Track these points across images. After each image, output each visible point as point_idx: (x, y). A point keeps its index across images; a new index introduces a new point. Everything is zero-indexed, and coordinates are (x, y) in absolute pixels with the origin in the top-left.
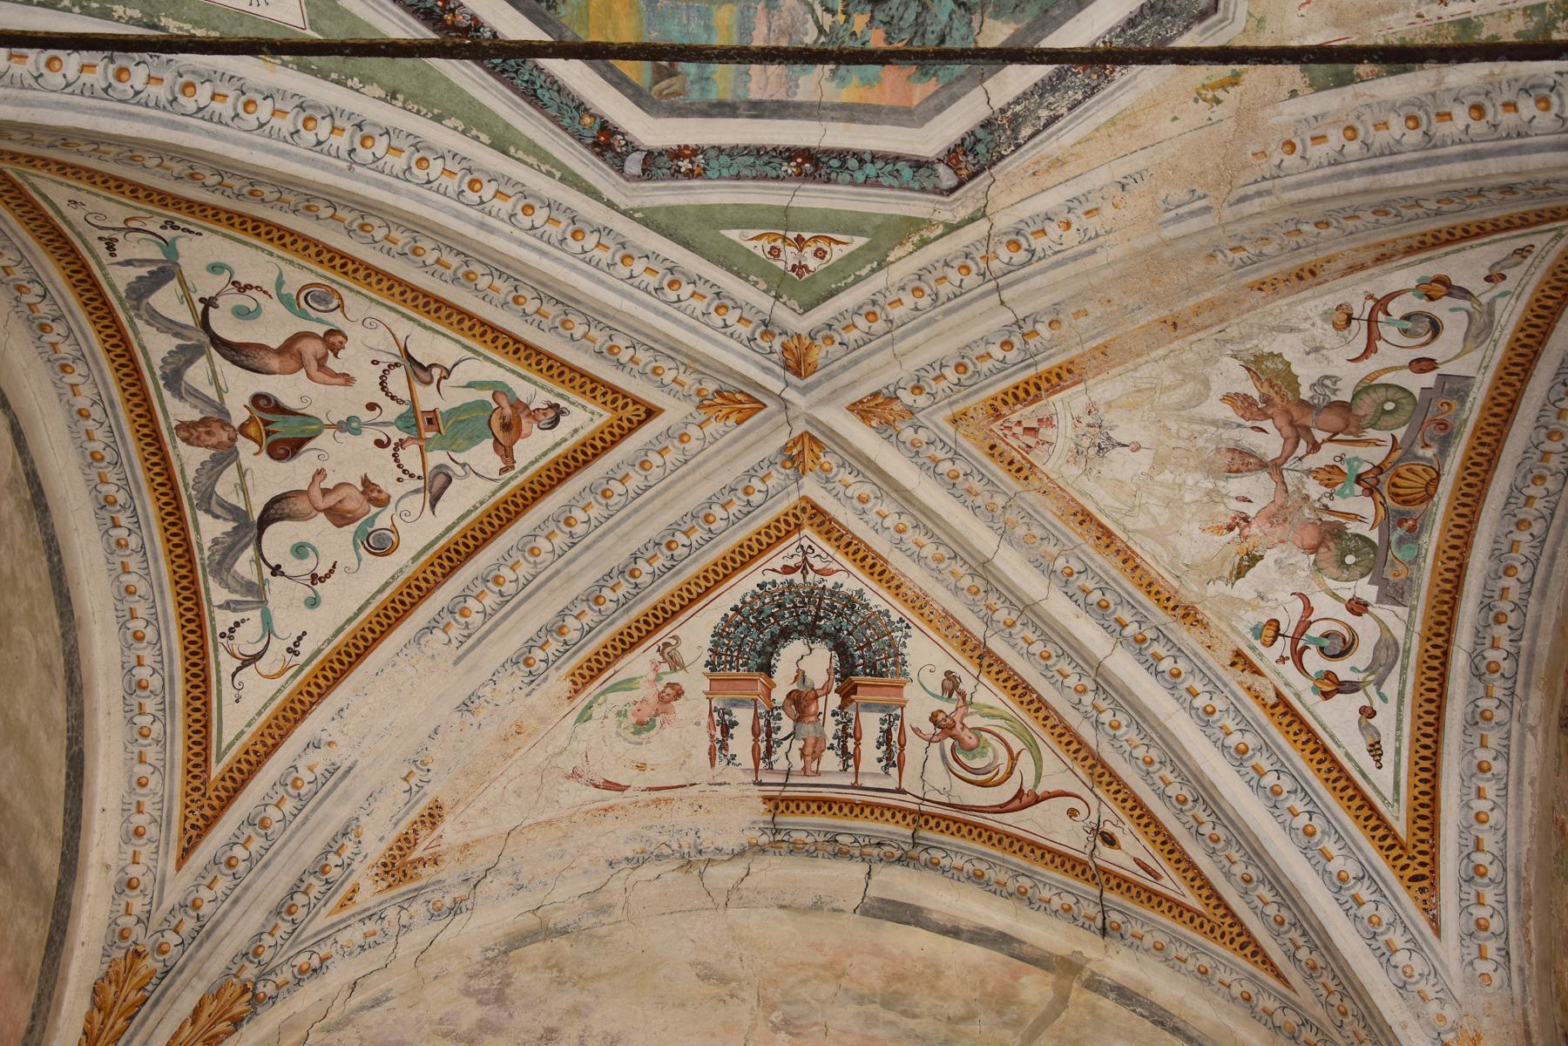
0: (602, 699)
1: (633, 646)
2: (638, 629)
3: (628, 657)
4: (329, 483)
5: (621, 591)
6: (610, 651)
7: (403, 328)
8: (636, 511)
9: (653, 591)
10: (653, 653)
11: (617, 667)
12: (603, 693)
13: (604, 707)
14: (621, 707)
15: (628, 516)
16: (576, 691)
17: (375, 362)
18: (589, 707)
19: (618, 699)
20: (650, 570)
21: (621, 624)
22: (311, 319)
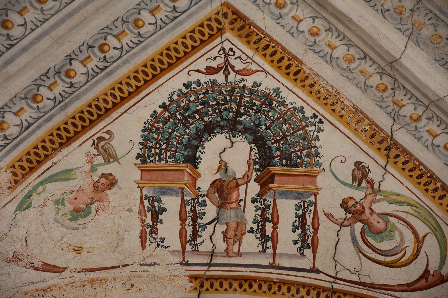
0: (40, 189)
1: (70, 140)
2: (74, 125)
3: (65, 151)
5: (57, 90)
6: (48, 145)
8: (70, 15)
9: (88, 90)
10: (88, 147)
11: (55, 159)
12: (42, 183)
13: (43, 196)
14: (59, 195)
15: (63, 21)
16: (16, 182)
18: (29, 196)
19: (55, 189)
20: (84, 70)
21: (58, 120)
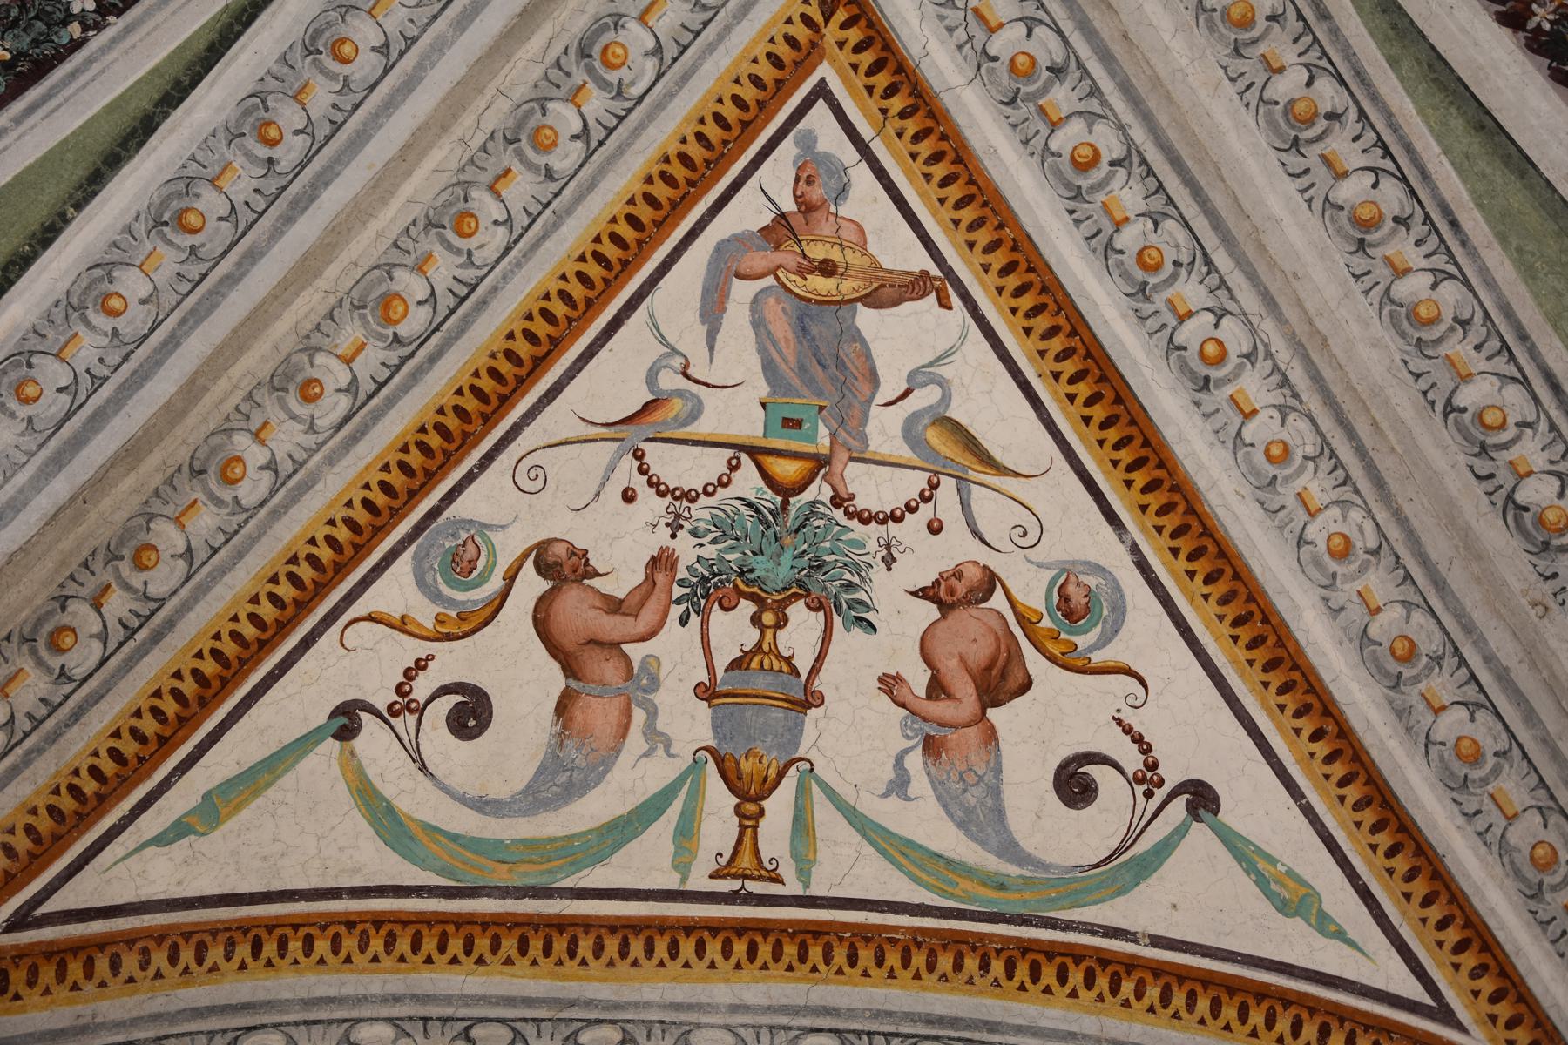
4: (918, 679)
7: (558, 420)
17: (628, 496)
22: (504, 595)
